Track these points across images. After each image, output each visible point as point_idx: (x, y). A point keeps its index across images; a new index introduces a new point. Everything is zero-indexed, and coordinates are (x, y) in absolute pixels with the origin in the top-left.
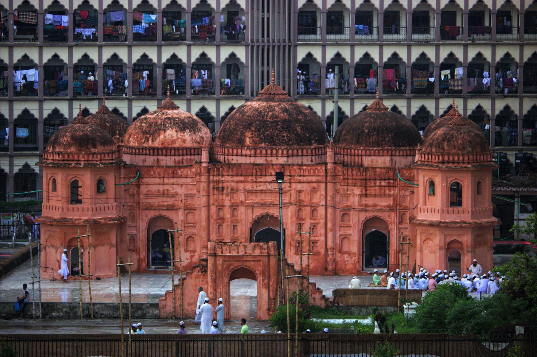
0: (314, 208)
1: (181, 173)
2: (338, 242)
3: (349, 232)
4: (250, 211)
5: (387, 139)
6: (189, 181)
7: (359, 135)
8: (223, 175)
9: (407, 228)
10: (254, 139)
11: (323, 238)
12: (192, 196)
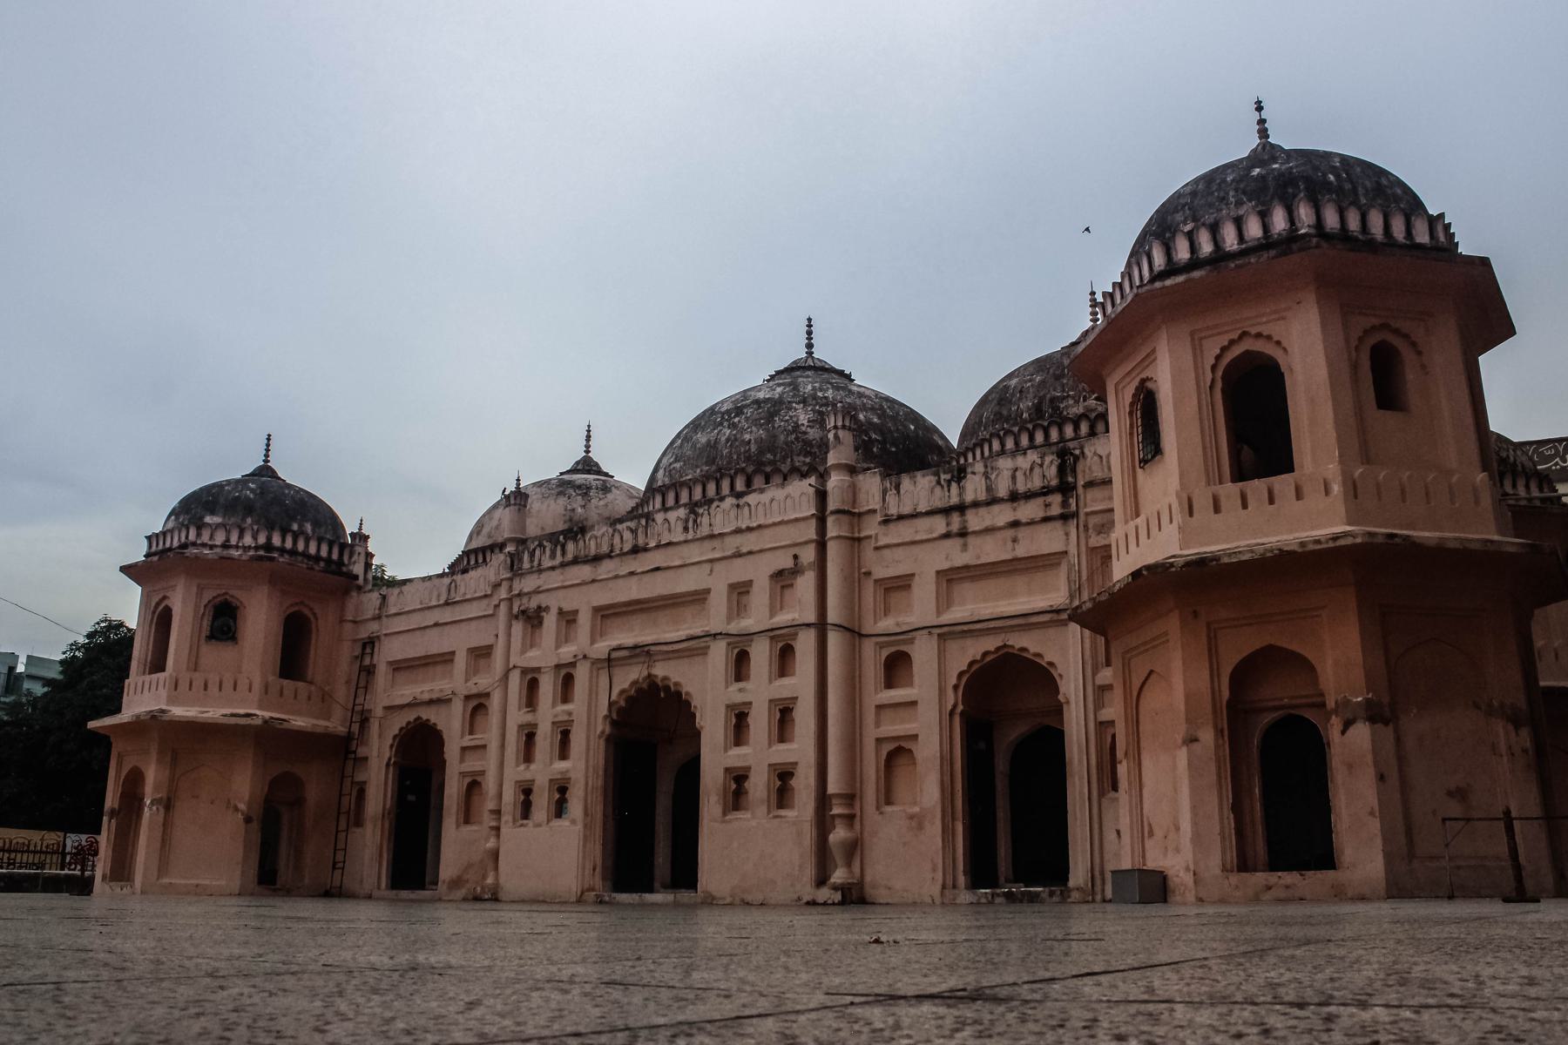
8: (540, 571)
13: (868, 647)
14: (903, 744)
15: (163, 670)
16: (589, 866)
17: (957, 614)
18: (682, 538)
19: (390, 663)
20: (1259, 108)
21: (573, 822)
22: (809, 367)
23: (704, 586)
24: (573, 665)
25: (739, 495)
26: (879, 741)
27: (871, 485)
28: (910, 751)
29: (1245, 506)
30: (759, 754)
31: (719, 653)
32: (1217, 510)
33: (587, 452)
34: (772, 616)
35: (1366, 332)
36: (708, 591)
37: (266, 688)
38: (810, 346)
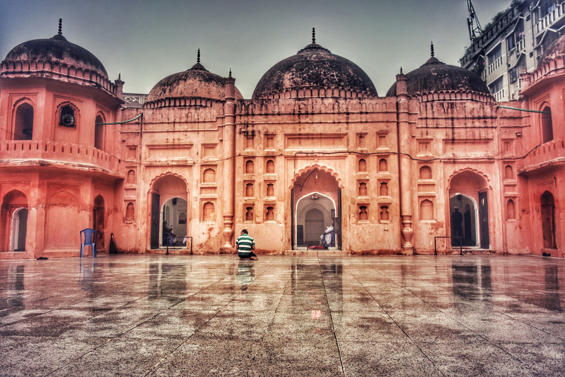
0: (383, 159)
1: (198, 115)
2: (417, 205)
3: (432, 193)
4: (291, 163)
5: (463, 81)
6: (208, 126)
7: (425, 79)
8: (253, 115)
9: (514, 186)
10: (295, 79)
11: (396, 200)
12: (211, 146)
13: (415, 162)
14: (428, 199)
16: (287, 240)
17: (449, 155)
18: (332, 111)
21: (279, 222)
22: (314, 47)
26: (419, 197)
28: (431, 202)
30: (373, 198)
31: (351, 160)
33: (199, 61)
34: (377, 147)
38: (314, 40)
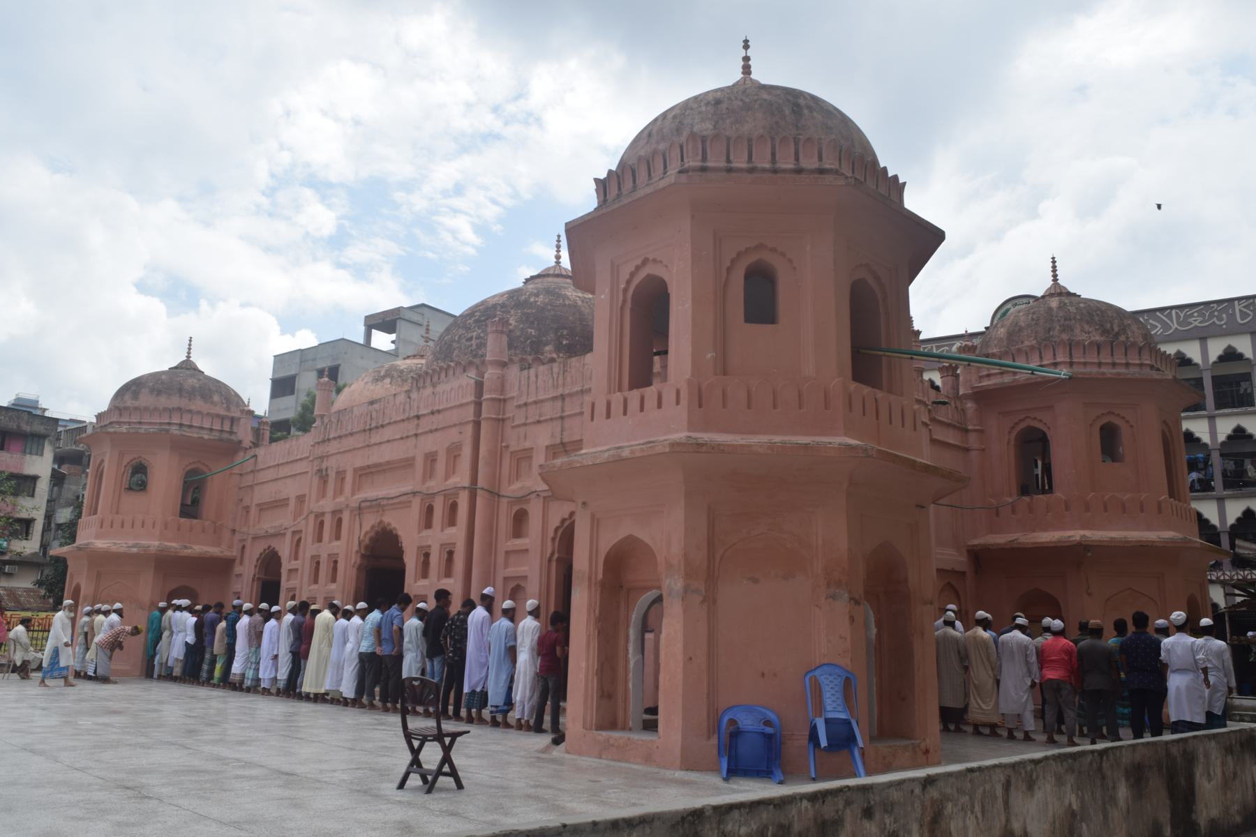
3: (522, 570)
13: (504, 501)
15: (95, 513)
19: (258, 505)
20: (746, 47)
23: (410, 455)
24: (340, 511)
25: (434, 386)
27: (513, 372)
29: (625, 414)
31: (416, 506)
32: (608, 416)
35: (739, 254)
36: (413, 458)
37: (166, 526)
